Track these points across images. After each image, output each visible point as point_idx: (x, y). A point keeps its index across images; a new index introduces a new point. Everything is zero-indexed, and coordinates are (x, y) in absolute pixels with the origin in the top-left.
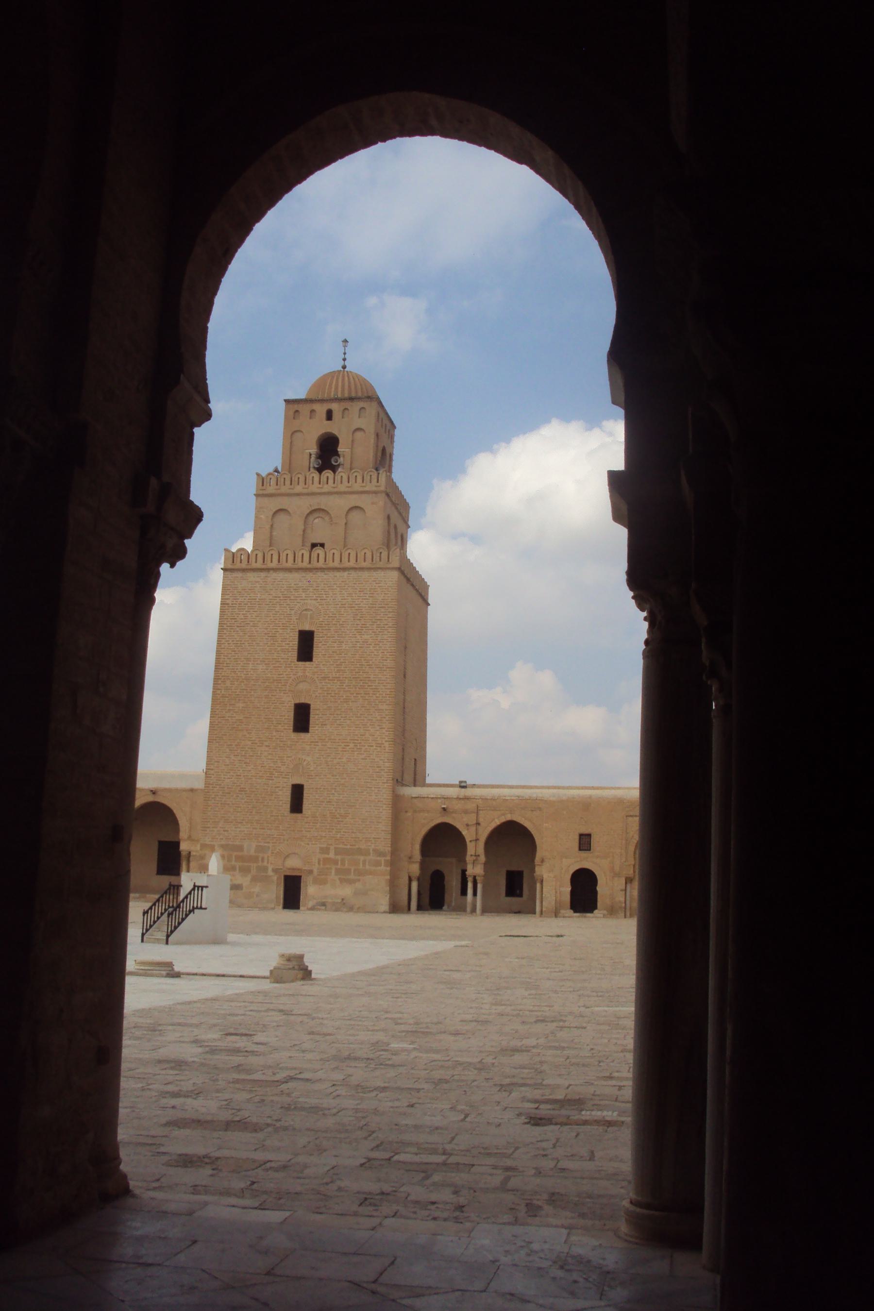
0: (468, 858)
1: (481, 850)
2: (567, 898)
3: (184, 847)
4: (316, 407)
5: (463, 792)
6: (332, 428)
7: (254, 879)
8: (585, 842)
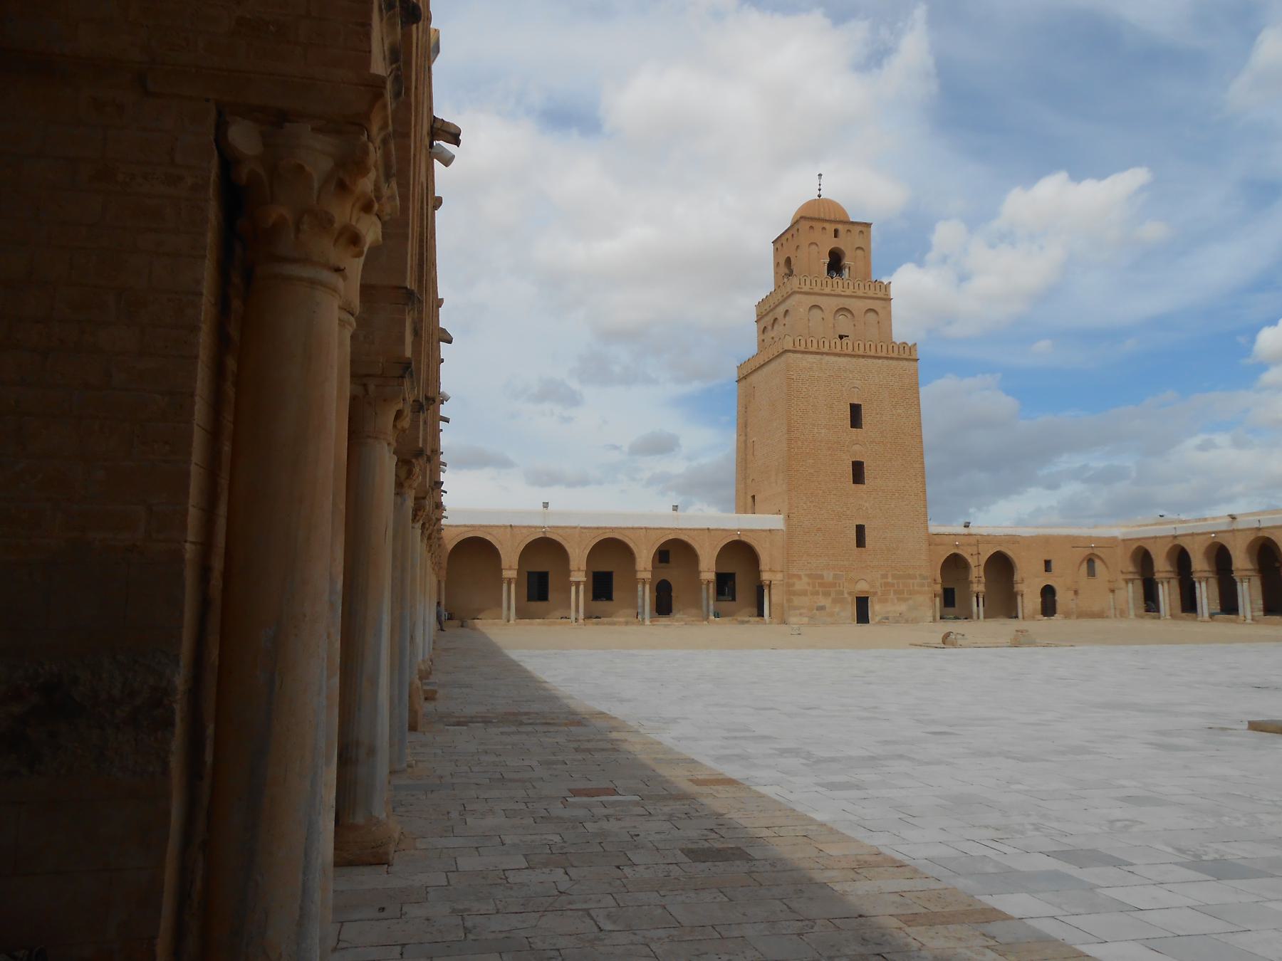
0: (975, 580)
1: (982, 574)
2: (1039, 607)
3: (765, 577)
4: (826, 225)
5: (965, 531)
6: (840, 243)
7: (835, 601)
8: (1048, 565)
